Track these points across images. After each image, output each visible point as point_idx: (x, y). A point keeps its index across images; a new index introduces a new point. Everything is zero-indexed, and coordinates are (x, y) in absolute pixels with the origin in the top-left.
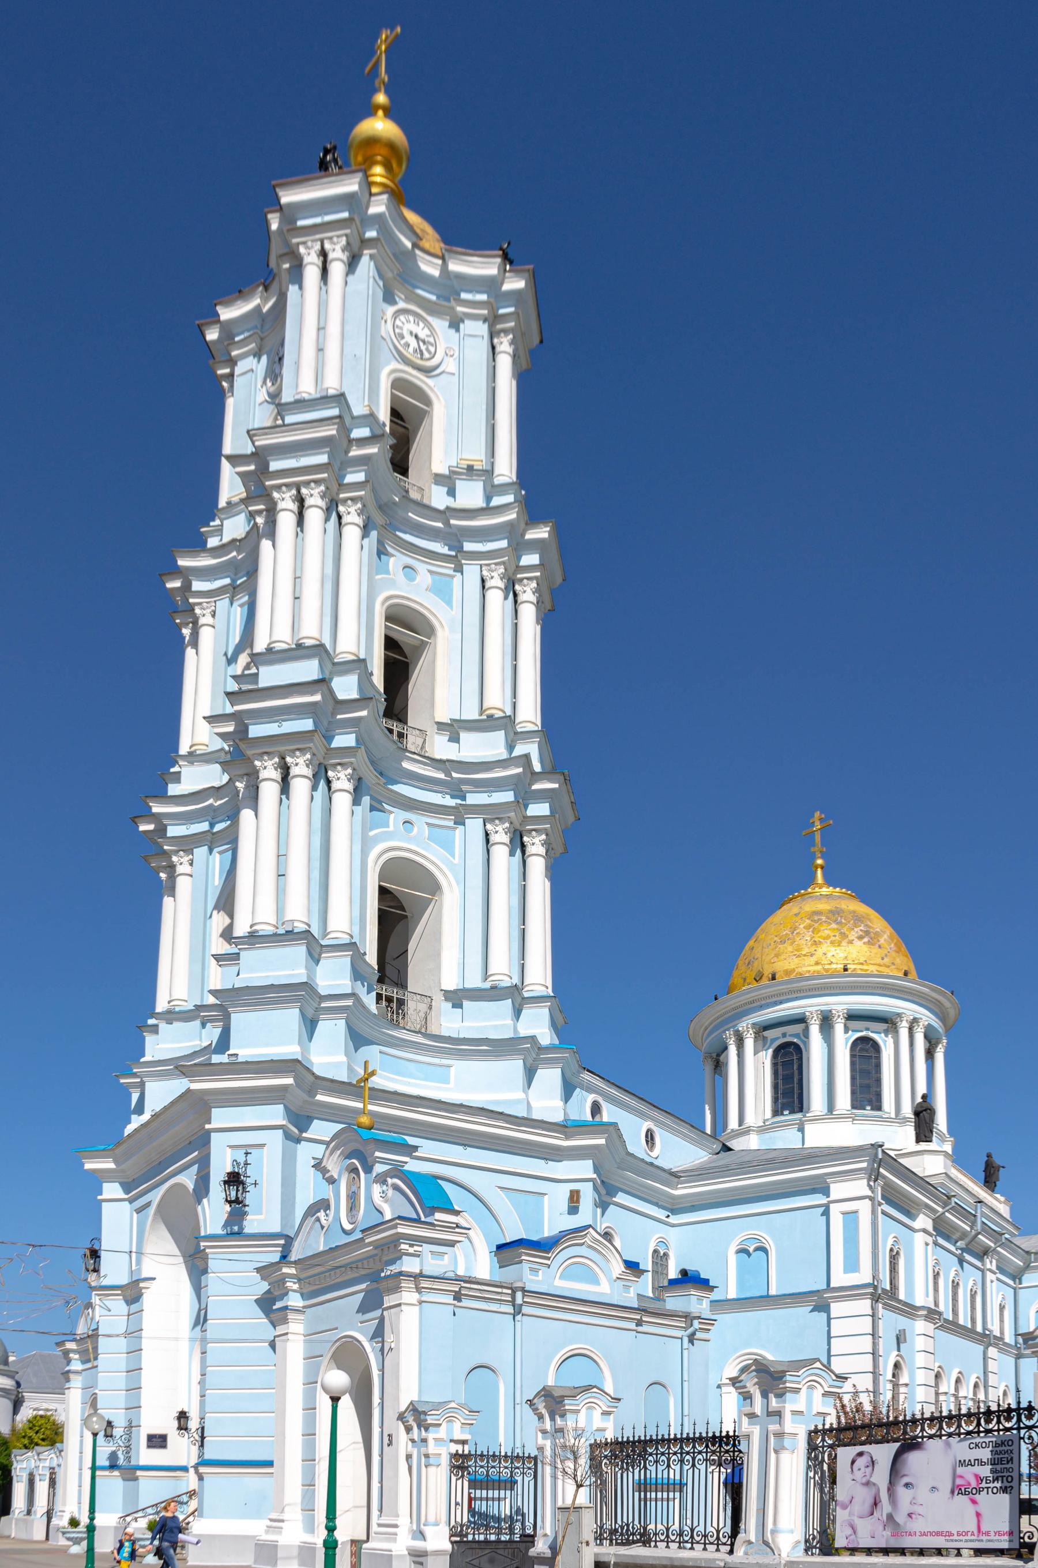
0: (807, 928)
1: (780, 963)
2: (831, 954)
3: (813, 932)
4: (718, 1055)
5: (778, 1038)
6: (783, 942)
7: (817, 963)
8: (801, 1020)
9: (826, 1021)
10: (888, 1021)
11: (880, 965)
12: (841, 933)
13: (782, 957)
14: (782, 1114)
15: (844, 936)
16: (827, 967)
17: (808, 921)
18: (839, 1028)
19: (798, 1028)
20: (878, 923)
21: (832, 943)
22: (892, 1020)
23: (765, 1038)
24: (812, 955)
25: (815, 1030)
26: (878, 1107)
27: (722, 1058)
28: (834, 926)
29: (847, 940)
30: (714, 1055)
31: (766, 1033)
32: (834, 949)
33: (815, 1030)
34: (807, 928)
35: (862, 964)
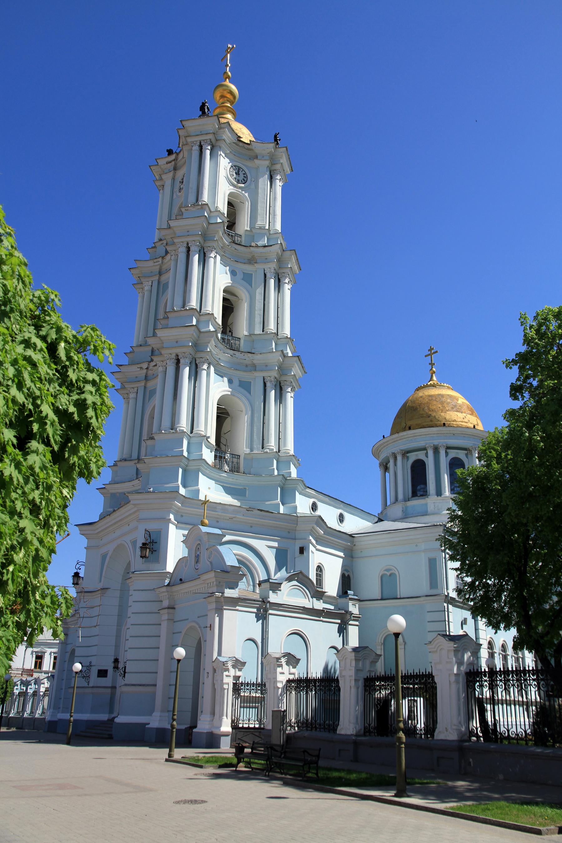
4: (387, 464)
8: (425, 449)
9: (436, 450)
18: (442, 452)
22: (469, 449)
25: (431, 453)
27: (388, 466)
30: (385, 464)
31: (408, 455)
35: (453, 421)
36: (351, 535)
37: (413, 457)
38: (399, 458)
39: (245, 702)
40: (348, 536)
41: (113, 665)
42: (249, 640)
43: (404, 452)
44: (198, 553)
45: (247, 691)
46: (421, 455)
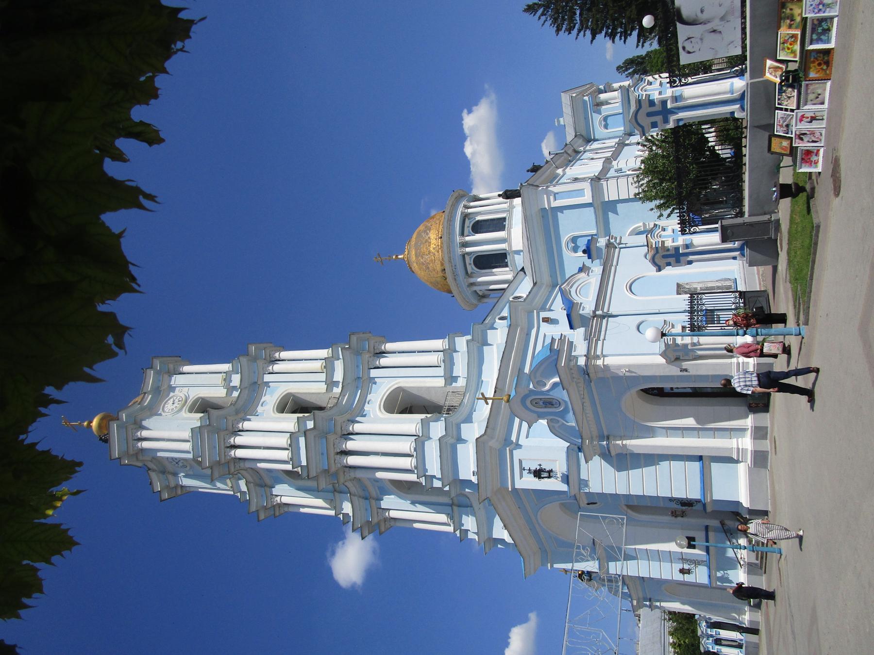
0: (422, 258)
1: (438, 269)
2: (434, 246)
3: (424, 255)
4: (479, 296)
5: (472, 267)
6: (428, 268)
7: (438, 252)
8: (463, 256)
9: (465, 245)
10: (465, 217)
11: (439, 224)
12: (425, 243)
13: (435, 268)
14: (507, 262)
15: (426, 241)
16: (440, 247)
17: (420, 258)
18: (468, 239)
19: (467, 258)
20: (421, 227)
21: (429, 246)
23: (472, 273)
24: (435, 254)
25: (468, 250)
26: (504, 219)
28: (422, 246)
29: (428, 240)
30: (479, 298)
31: (469, 273)
32: (432, 245)
33: (468, 250)
34: (422, 258)
36: (535, 284)
37: (471, 268)
38: (472, 280)
39: (713, 319)
40: (535, 287)
41: (679, 519)
42: (639, 331)
43: (466, 277)
44: (541, 404)
45: (699, 307)
46: (469, 261)
